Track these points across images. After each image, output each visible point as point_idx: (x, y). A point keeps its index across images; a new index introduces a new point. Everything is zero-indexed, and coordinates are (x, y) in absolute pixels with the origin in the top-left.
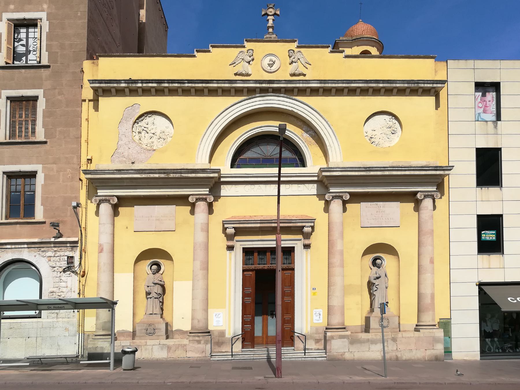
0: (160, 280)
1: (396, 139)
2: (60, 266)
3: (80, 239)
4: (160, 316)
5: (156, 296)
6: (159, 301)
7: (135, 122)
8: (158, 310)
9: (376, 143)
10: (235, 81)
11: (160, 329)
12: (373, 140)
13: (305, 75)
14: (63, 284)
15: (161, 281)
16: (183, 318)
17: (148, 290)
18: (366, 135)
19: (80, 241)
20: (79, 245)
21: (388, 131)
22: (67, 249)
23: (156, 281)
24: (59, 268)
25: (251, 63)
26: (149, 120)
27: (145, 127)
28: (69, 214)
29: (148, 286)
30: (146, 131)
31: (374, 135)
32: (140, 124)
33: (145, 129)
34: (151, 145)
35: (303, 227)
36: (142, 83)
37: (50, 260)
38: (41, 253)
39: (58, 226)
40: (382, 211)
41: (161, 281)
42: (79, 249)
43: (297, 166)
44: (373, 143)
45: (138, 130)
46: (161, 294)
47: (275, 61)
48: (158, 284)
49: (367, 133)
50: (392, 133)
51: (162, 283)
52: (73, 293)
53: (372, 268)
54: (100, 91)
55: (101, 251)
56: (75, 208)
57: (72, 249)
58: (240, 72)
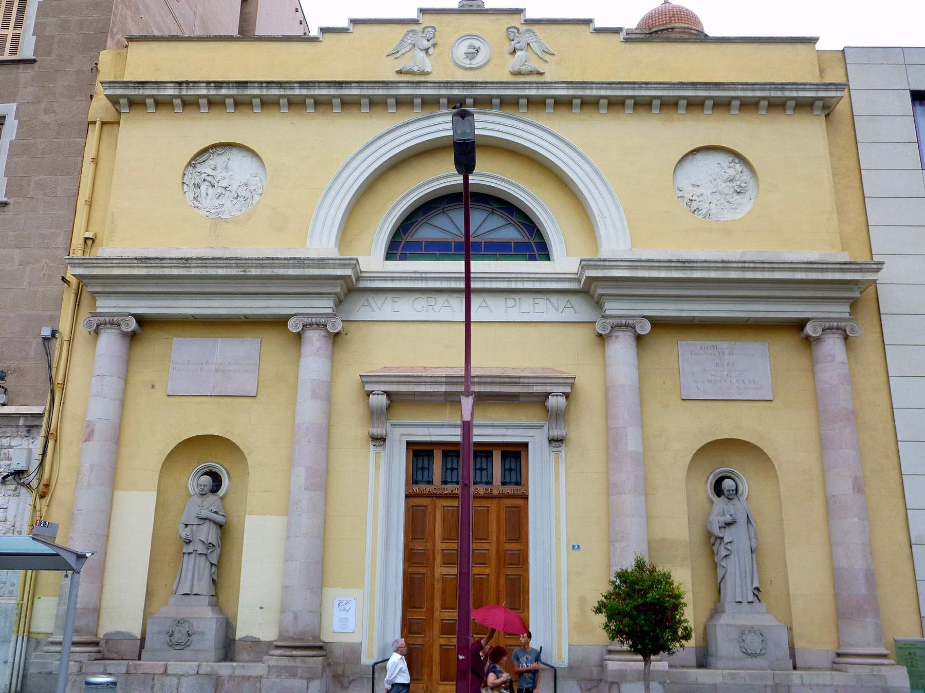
1: (746, 205)
3: (47, 409)
4: (205, 600)
5: (201, 549)
6: (208, 564)
7: (189, 164)
8: (203, 586)
9: (704, 211)
11: (203, 634)
12: (695, 205)
13: (540, 74)
15: (216, 512)
16: (261, 608)
17: (184, 533)
18: (680, 194)
19: (47, 414)
21: (728, 188)
22: (18, 431)
23: (205, 513)
25: (431, 51)
26: (218, 160)
27: (208, 175)
28: (32, 354)
29: (187, 525)
30: (210, 182)
31: (698, 194)
32: (200, 168)
33: (207, 178)
34: (218, 210)
35: (547, 395)
36: (208, 88)
41: (216, 512)
42: (43, 429)
43: (532, 258)
44: (695, 211)
47: (479, 48)
48: (210, 520)
49: (681, 191)
50: (736, 191)
51: (219, 519)
53: (714, 499)
54: (124, 101)
55: (89, 437)
56: (45, 339)
57: (29, 431)
58: (409, 68)
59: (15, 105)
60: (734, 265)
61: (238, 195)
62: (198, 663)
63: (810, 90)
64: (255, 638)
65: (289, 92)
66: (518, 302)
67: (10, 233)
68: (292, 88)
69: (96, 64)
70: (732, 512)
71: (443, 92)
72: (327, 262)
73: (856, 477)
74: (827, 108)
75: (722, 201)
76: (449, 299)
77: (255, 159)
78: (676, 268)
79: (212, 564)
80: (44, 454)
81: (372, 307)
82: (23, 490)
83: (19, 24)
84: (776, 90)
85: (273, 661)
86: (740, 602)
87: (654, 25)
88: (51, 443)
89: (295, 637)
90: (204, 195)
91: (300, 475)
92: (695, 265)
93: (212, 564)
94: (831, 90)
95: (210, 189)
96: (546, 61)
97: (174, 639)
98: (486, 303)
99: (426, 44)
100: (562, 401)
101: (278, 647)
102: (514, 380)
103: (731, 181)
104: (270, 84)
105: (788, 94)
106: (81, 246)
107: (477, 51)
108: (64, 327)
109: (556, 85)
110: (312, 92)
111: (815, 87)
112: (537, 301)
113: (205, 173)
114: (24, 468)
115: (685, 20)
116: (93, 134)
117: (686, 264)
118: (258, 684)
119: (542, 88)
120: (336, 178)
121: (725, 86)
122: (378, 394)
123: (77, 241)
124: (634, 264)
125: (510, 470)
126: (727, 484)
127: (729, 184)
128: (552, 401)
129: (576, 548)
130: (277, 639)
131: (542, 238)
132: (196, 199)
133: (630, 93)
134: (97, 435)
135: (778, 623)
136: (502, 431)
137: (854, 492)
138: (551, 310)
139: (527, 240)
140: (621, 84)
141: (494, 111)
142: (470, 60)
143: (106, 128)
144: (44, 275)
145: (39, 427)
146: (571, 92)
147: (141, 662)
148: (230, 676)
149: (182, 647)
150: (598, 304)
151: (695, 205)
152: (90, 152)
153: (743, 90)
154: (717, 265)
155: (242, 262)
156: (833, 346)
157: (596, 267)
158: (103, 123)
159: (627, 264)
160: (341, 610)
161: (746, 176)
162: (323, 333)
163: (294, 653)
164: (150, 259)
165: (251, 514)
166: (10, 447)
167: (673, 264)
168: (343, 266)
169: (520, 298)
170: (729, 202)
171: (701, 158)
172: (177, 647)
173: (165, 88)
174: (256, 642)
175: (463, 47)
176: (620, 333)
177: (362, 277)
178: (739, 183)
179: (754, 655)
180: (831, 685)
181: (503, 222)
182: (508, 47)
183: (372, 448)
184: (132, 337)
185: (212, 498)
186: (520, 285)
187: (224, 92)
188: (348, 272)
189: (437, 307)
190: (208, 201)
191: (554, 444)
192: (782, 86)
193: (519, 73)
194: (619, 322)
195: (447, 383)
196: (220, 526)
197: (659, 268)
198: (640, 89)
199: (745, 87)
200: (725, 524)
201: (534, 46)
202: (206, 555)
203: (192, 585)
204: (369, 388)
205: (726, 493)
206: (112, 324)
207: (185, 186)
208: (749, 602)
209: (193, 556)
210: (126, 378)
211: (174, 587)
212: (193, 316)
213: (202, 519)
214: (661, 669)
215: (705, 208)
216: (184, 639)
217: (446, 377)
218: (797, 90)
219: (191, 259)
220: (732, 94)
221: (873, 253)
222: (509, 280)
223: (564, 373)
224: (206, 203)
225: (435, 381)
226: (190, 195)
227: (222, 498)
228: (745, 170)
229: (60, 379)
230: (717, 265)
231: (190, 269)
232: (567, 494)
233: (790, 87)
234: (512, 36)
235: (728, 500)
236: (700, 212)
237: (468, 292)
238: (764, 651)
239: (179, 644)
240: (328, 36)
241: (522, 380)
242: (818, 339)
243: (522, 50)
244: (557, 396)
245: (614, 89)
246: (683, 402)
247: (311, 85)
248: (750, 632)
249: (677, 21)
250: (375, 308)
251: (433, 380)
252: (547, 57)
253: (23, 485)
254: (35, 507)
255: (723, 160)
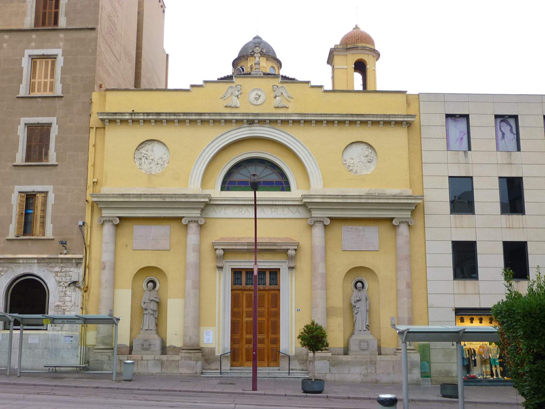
0: (155, 297)
1: (372, 168)
2: (66, 281)
3: (84, 256)
4: (155, 332)
5: (151, 312)
6: (154, 318)
7: (137, 149)
8: (153, 327)
9: (354, 171)
10: (224, 114)
12: (351, 168)
14: (68, 299)
15: (156, 298)
16: (176, 335)
17: (144, 306)
18: (345, 162)
19: (84, 258)
20: (84, 261)
21: (365, 160)
22: (72, 265)
23: (152, 298)
24: (64, 283)
25: (239, 96)
26: (148, 147)
27: (145, 154)
29: (144, 303)
31: (352, 163)
32: (141, 150)
33: (144, 155)
34: (150, 170)
35: (288, 250)
37: (57, 275)
38: (49, 268)
39: (66, 244)
40: (362, 236)
41: (156, 298)
42: (83, 264)
44: (351, 170)
45: (138, 157)
46: (156, 311)
48: (154, 301)
49: (345, 161)
51: (157, 300)
52: (76, 307)
53: (354, 290)
56: (80, 226)
57: (77, 265)
58: (230, 105)
59: (56, 118)
60: (364, 197)
61: (158, 163)
62: (154, 356)
63: (401, 117)
64: (174, 346)
65: (179, 118)
66: (276, 210)
67: (60, 178)
68: (180, 116)
69: (91, 99)
70: (360, 296)
71: (245, 118)
72: (198, 196)
73: (408, 282)
74: (409, 124)
75: (363, 165)
76: (248, 208)
77: (164, 146)
78: (340, 198)
79: (155, 318)
80: (85, 274)
81: (216, 212)
82: (77, 289)
83: (52, 76)
84: (387, 117)
85: (183, 355)
86: (361, 330)
87: (349, 43)
88: (87, 270)
89: (191, 345)
90: (143, 163)
91: (189, 283)
92: (348, 197)
93: (155, 318)
94: (409, 117)
95: (146, 160)
96: (289, 101)
97: (144, 347)
98: (263, 210)
99: (237, 93)
100: (293, 252)
101: (183, 349)
102: (274, 244)
103: (367, 156)
104: (170, 114)
105: (391, 119)
106: (92, 185)
107: (259, 96)
108: (88, 220)
109: (293, 115)
110: (189, 118)
111: (403, 116)
112: (284, 209)
113: (143, 153)
114: (77, 280)
115: (364, 41)
116: (93, 133)
117: (344, 197)
118: (177, 363)
119: (287, 116)
120: (200, 156)
121: (365, 116)
122: (220, 250)
123: (90, 183)
124: (324, 196)
125: (273, 279)
126: (359, 285)
127: (366, 158)
128: (290, 252)
129: (299, 310)
130: (182, 346)
131: (287, 179)
132: (140, 165)
133: (325, 118)
134: (107, 267)
135: (374, 338)
136: (270, 264)
137: (406, 288)
138: (290, 213)
139: (280, 180)
140: (321, 115)
141: (267, 126)
142: (257, 101)
143: (98, 130)
144: (77, 197)
145: (81, 263)
146: (300, 118)
147: (132, 355)
148: (167, 360)
149: (147, 350)
150: (309, 211)
151: (351, 168)
152: (92, 142)
153: (372, 117)
154: (357, 197)
155: (163, 196)
156: (403, 229)
157: (308, 198)
158: (96, 128)
159: (320, 196)
160: (207, 335)
161: (373, 154)
162: (196, 224)
163: (191, 351)
164: (125, 194)
165: (169, 298)
166: (70, 271)
167: (339, 197)
168: (205, 198)
169: (277, 208)
170: (365, 166)
171: (354, 145)
172: (145, 350)
173: (125, 116)
174: (175, 347)
175: (253, 95)
176: (318, 224)
177: (212, 200)
178: (370, 158)
179: (363, 350)
180: (391, 360)
181: (272, 172)
182: (273, 95)
183: (217, 271)
184: (117, 226)
185: (153, 292)
186: (277, 203)
187: (150, 117)
188: (207, 200)
189: (243, 212)
190: (145, 166)
191: (290, 269)
192: (389, 116)
193: (277, 107)
194: (317, 220)
195: (247, 245)
196: (157, 303)
197: (333, 198)
198: (329, 117)
199: (373, 116)
200: (357, 300)
201: (285, 94)
202: (153, 314)
203: (149, 326)
204: (216, 247)
205: (358, 288)
206: (109, 221)
207: (135, 159)
208: (364, 331)
209: (148, 315)
210: (115, 243)
211: (141, 327)
212: (142, 217)
213: (151, 300)
214: (328, 355)
215: (355, 169)
216: (148, 347)
217: (247, 243)
218: (395, 117)
219: (142, 195)
220: (368, 119)
221: (424, 188)
222: (273, 201)
223: (294, 240)
224: (145, 167)
225: (242, 244)
226: (137, 163)
227: (157, 291)
228: (373, 151)
229: (88, 243)
230: (357, 197)
231: (141, 199)
232: (296, 289)
233: (392, 116)
234: (275, 89)
235: (358, 291)
236: (353, 171)
237: (255, 205)
238: (367, 349)
239: (146, 349)
240: (194, 88)
241: (278, 244)
242: (398, 226)
243: (279, 96)
244: (292, 250)
245: (318, 117)
246: (343, 252)
247: (188, 114)
248: (363, 342)
249: (360, 42)
250: (217, 212)
251: (242, 244)
252: (290, 100)
253: (77, 287)
254: (83, 296)
255: (364, 147)
